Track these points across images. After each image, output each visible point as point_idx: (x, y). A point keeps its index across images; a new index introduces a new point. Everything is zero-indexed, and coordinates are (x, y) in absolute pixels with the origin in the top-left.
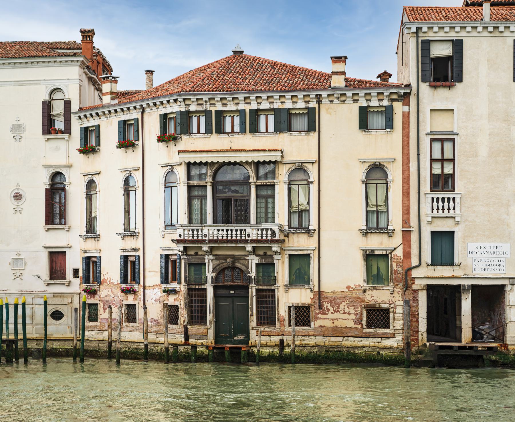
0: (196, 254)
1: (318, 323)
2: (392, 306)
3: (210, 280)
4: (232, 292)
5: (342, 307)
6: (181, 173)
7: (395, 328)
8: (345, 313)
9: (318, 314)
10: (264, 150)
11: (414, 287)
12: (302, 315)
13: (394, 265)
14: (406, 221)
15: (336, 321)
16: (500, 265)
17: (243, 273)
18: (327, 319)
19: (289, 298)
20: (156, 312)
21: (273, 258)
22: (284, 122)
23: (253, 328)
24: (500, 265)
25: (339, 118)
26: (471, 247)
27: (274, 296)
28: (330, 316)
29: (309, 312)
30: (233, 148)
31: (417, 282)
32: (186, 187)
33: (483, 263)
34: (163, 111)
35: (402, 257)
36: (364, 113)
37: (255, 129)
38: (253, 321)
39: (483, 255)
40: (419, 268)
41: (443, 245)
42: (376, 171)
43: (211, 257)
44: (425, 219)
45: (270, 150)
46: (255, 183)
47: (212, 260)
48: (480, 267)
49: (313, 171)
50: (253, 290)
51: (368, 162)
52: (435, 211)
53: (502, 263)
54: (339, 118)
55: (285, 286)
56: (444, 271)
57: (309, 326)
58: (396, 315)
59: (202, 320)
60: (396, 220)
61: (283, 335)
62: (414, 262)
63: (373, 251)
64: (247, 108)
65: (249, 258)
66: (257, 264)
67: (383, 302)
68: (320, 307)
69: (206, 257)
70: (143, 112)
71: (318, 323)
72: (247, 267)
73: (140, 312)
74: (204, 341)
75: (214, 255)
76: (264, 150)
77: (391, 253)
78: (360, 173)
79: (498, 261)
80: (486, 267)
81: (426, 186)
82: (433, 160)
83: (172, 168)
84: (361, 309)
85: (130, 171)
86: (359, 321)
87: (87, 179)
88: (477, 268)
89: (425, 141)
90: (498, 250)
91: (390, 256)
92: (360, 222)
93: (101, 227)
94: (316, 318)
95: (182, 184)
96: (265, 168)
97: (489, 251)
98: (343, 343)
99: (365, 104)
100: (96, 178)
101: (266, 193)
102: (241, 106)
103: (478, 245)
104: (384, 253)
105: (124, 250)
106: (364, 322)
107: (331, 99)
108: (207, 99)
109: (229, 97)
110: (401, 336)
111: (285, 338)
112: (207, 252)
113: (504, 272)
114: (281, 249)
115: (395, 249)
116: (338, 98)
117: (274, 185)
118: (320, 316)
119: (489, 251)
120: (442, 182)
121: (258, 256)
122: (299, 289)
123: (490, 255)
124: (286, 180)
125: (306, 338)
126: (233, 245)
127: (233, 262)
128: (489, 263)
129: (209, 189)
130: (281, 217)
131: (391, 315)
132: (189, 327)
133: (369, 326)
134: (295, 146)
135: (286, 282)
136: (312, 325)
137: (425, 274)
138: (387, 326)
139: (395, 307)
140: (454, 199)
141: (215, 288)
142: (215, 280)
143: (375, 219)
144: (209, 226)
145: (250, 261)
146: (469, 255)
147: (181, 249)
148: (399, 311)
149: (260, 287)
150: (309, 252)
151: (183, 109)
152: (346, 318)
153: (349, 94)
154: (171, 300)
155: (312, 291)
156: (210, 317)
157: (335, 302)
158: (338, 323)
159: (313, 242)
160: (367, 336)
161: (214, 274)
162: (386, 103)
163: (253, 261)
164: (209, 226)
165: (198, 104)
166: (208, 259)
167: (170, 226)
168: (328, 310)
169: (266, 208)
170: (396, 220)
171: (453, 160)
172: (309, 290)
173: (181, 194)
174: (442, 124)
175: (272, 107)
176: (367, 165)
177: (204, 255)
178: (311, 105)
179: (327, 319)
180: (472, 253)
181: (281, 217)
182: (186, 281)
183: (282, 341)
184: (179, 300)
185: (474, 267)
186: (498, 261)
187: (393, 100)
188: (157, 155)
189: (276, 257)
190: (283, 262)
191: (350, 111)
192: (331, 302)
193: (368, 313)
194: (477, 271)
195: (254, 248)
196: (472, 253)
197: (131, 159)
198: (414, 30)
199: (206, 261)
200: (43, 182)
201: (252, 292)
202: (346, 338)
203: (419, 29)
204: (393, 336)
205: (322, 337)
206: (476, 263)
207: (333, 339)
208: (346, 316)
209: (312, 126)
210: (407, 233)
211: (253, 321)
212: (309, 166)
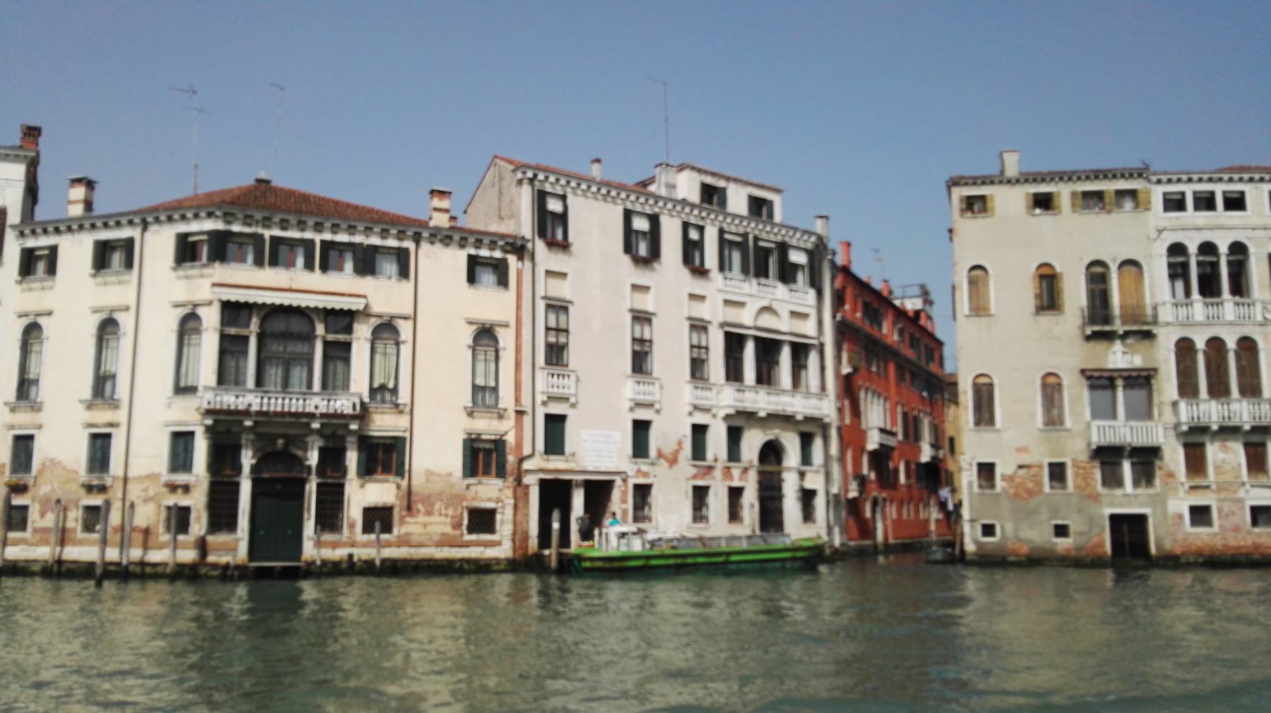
0: (229, 431)
1: (404, 529)
5: (437, 506)
6: (211, 317)
8: (440, 515)
10: (342, 295)
14: (518, 400)
17: (300, 462)
19: (362, 494)
20: (147, 515)
22: (367, 262)
23: (309, 539)
25: (441, 266)
26: (584, 434)
27: (342, 493)
28: (421, 518)
30: (294, 287)
34: (183, 228)
36: (473, 262)
42: (485, 334)
43: (251, 437)
44: (540, 398)
45: (350, 295)
46: (324, 337)
49: (405, 328)
54: (441, 266)
56: (556, 463)
59: (231, 526)
61: (353, 546)
62: (527, 450)
64: (318, 238)
67: (489, 500)
68: (409, 508)
69: (244, 436)
70: (145, 229)
71: (404, 529)
73: (115, 518)
76: (342, 295)
78: (468, 334)
82: (548, 329)
87: (25, 321)
89: (541, 305)
93: (45, 392)
94: (402, 522)
96: (343, 319)
99: (473, 252)
100: (42, 321)
101: (339, 352)
102: (308, 235)
109: (293, 220)
118: (408, 519)
120: (556, 354)
124: (369, 335)
126: (293, 420)
127: (286, 445)
130: (359, 382)
131: (498, 517)
134: (382, 294)
136: (396, 531)
137: (539, 465)
139: (503, 507)
141: (256, 482)
142: (254, 469)
143: (483, 396)
144: (251, 391)
148: (509, 512)
151: (219, 225)
153: (456, 237)
157: (429, 501)
158: (431, 529)
159: (403, 421)
160: (467, 545)
161: (254, 461)
162: (498, 254)
167: (183, 389)
168: (418, 511)
170: (506, 398)
171: (567, 331)
173: (209, 344)
174: (561, 290)
176: (474, 327)
181: (359, 382)
183: (351, 556)
187: (506, 252)
188: (162, 287)
192: (422, 501)
197: (115, 292)
198: (530, 174)
199: (243, 442)
203: (535, 175)
204: (499, 543)
208: (443, 519)
209: (404, 273)
210: (520, 413)
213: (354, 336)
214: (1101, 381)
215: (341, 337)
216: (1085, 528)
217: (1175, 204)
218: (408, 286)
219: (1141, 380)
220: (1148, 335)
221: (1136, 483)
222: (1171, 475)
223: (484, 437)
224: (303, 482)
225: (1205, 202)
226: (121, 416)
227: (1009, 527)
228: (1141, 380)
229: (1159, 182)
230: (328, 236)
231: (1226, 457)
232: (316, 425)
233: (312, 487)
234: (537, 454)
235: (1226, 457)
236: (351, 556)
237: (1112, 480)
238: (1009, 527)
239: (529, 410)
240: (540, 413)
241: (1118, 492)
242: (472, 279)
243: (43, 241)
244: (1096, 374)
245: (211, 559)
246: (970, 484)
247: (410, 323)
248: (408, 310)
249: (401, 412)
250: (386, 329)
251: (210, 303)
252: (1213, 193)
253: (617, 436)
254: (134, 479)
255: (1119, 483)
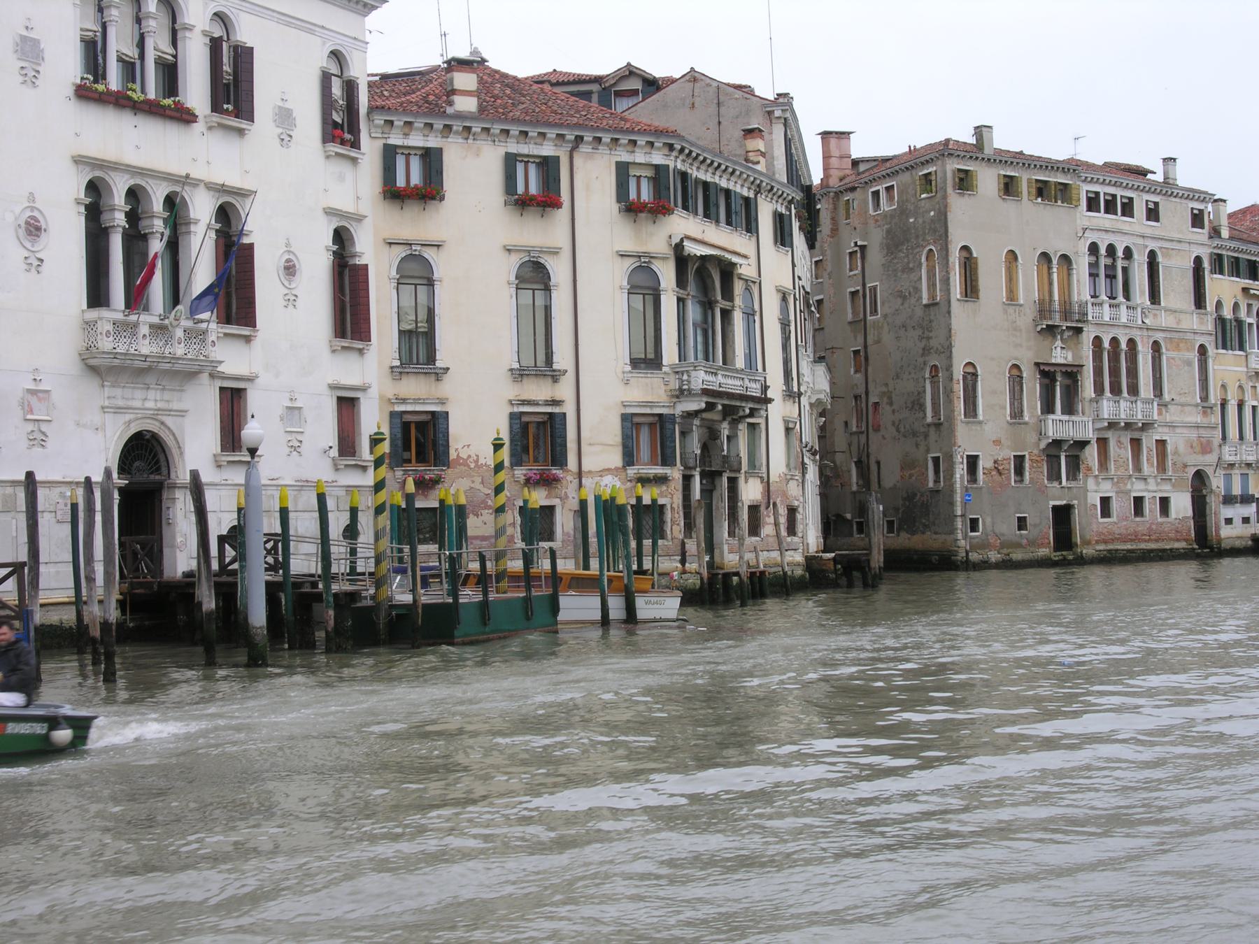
30: (706, 239)
214: (1047, 374)
216: (1038, 521)
217: (1092, 204)
219: (1072, 374)
220: (1078, 331)
221: (1068, 479)
222: (1089, 469)
225: (1110, 207)
226: (564, 391)
227: (988, 520)
228: (1072, 374)
229: (1084, 181)
231: (1120, 450)
235: (1120, 450)
237: (1054, 475)
238: (988, 520)
241: (1056, 484)
244: (1047, 369)
246: (962, 476)
252: (1114, 196)
254: (590, 472)
255: (1059, 478)
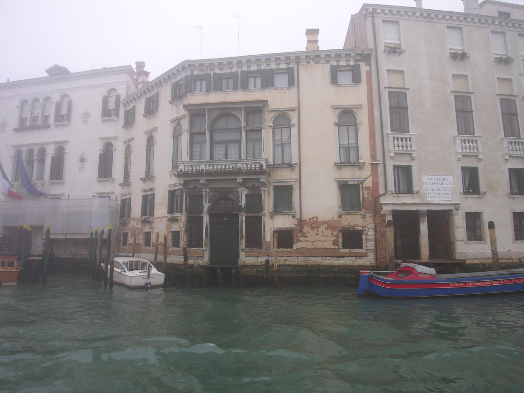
2: (364, 228)
3: (206, 209)
4: (225, 219)
6: (185, 124)
7: (368, 248)
8: (323, 236)
9: (300, 237)
11: (383, 213)
12: (285, 238)
13: (366, 193)
14: (373, 157)
15: (315, 243)
16: (447, 194)
18: (307, 241)
19: (273, 223)
21: (260, 190)
23: (242, 250)
24: (447, 194)
26: (425, 178)
29: (291, 235)
31: (385, 208)
32: (189, 134)
33: (434, 192)
35: (371, 186)
37: (245, 87)
38: (243, 244)
39: (434, 185)
40: (386, 196)
41: (405, 177)
43: (208, 190)
46: (245, 128)
47: (209, 192)
48: (433, 195)
50: (243, 218)
51: (340, 108)
52: (397, 148)
53: (448, 192)
55: (271, 213)
57: (292, 248)
58: (368, 237)
60: (365, 156)
61: (268, 256)
62: (382, 191)
63: (347, 181)
65: (240, 190)
66: (246, 195)
69: (204, 190)
72: (238, 197)
74: (200, 262)
75: (210, 188)
77: (362, 183)
79: (445, 190)
80: (437, 195)
81: (388, 130)
83: (179, 121)
84: (338, 232)
85: (151, 131)
86: (335, 243)
87: (126, 145)
88: (430, 195)
90: (445, 182)
91: (361, 186)
92: (335, 157)
95: (186, 132)
97: (438, 182)
98: (322, 262)
99: (335, 64)
103: (430, 177)
104: (356, 183)
105: (145, 191)
106: (340, 244)
107: (307, 60)
108: (208, 64)
110: (373, 255)
111: (270, 259)
112: (203, 184)
113: (450, 199)
114: (268, 181)
115: (366, 179)
116: (313, 59)
117: (260, 130)
118: (301, 239)
119: (438, 182)
121: (247, 188)
122: (283, 216)
123: (439, 186)
125: (289, 258)
128: (439, 192)
129: (208, 135)
131: (364, 236)
132: (188, 249)
133: (344, 247)
135: (271, 210)
136: (294, 248)
137: (390, 202)
138: (361, 247)
140: (410, 139)
141: (211, 216)
145: (240, 192)
146: (424, 185)
147: (182, 182)
148: (371, 234)
149: (249, 215)
150: (291, 184)
152: (325, 240)
154: (175, 227)
155: (294, 217)
156: (205, 240)
158: (317, 245)
162: (352, 63)
163: (243, 193)
164: (207, 162)
165: (200, 70)
166: (205, 192)
169: (254, 149)
170: (365, 156)
172: (291, 217)
175: (259, 68)
176: (338, 111)
177: (202, 189)
178: (291, 66)
179: (307, 241)
180: (426, 183)
182: (186, 210)
183: (267, 261)
184: (180, 227)
185: (428, 195)
186: (445, 190)
189: (262, 188)
190: (269, 193)
191: (323, 71)
193: (343, 235)
194: (430, 199)
195: (244, 180)
196: (426, 183)
199: (204, 193)
200: (98, 148)
201: (242, 219)
202: (324, 258)
204: (364, 255)
205: (303, 258)
206: (429, 192)
207: (312, 259)
208: (325, 238)
210: (374, 166)
211: (243, 244)
212: (291, 113)
213: (263, 126)
215: (256, 127)
218: (294, 91)
223: (350, 183)
224: (237, 216)
230: (245, 69)
232: (240, 180)
233: (243, 218)
234: (389, 192)
236: (267, 261)
239: (381, 163)
240: (390, 165)
242: (334, 80)
243: (131, 106)
245: (190, 261)
247: (296, 113)
248: (294, 105)
249: (293, 170)
250: (283, 119)
251: (184, 117)
253: (450, 179)
